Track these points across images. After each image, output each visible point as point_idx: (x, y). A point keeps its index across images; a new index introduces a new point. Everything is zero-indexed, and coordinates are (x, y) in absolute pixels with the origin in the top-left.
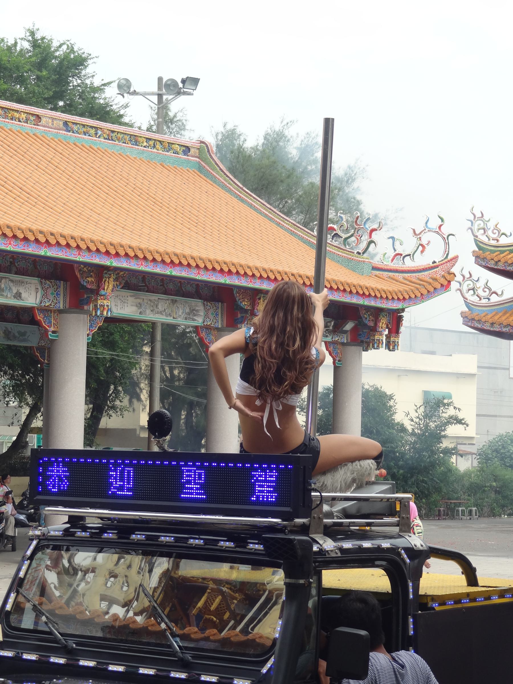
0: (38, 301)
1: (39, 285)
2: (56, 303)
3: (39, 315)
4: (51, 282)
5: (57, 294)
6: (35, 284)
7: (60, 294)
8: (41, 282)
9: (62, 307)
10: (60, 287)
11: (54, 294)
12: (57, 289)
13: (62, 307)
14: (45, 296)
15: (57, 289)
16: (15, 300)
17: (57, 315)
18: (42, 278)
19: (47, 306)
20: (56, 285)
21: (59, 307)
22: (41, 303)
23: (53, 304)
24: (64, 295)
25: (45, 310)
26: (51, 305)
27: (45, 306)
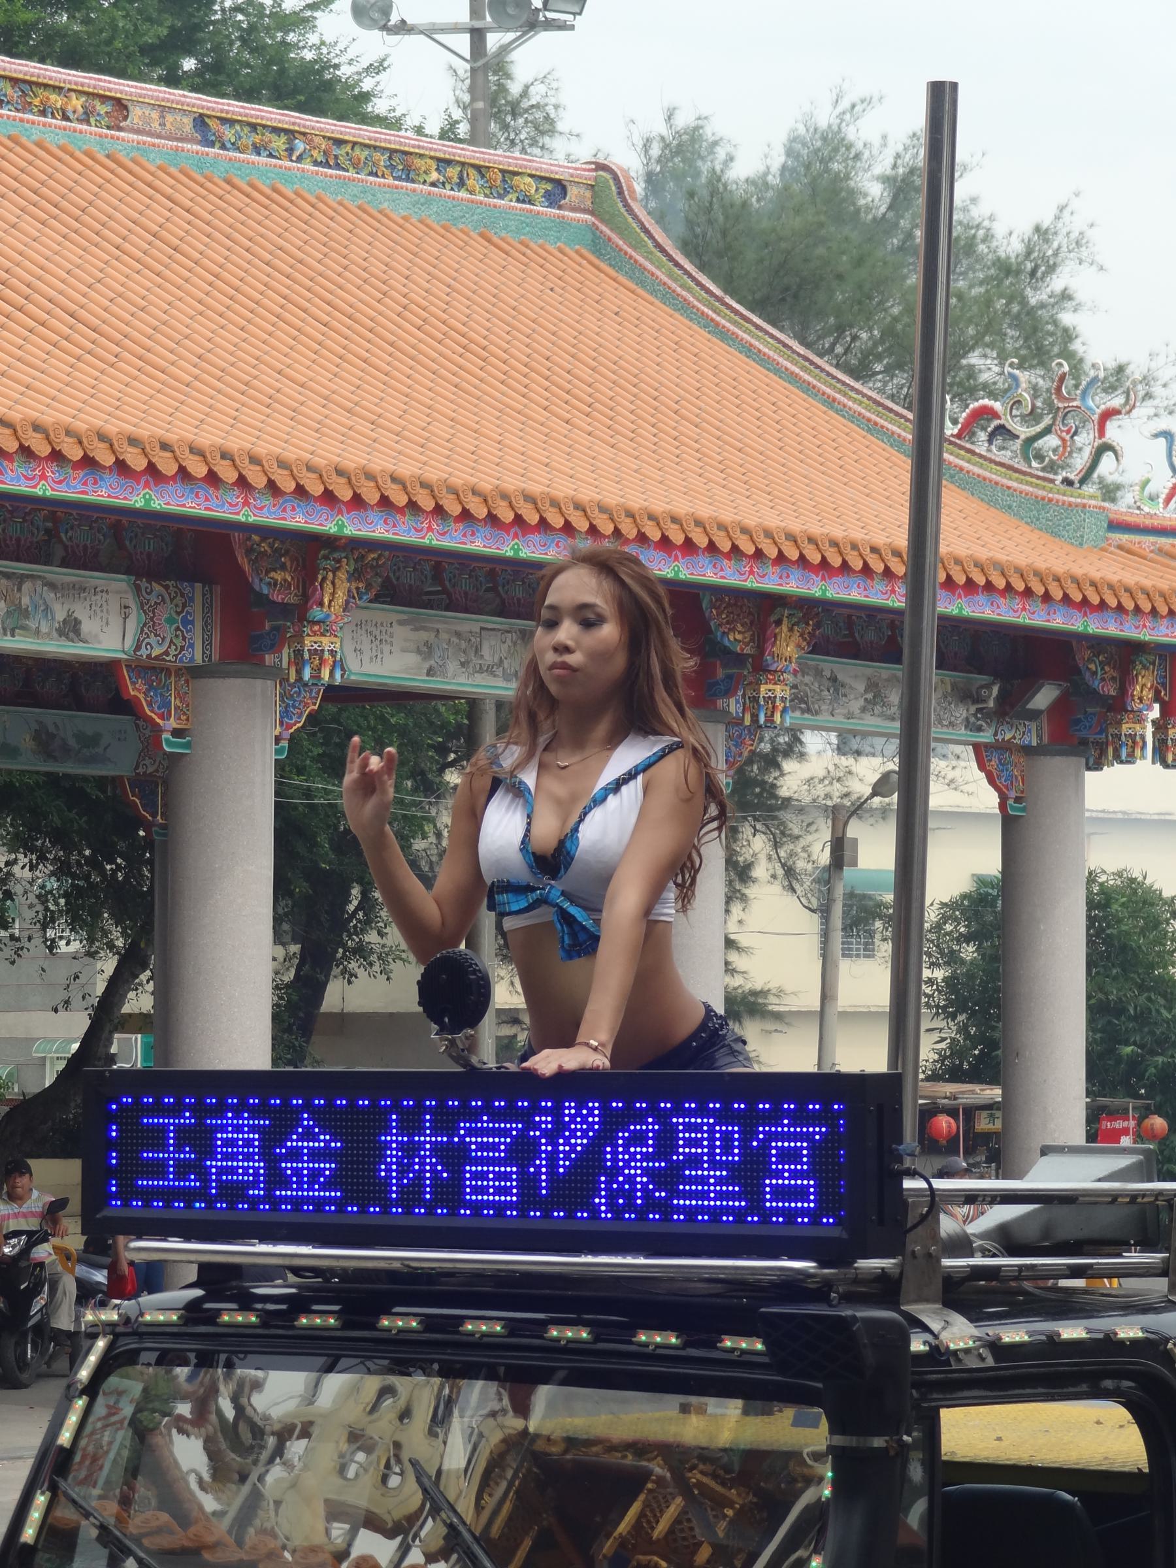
0: (129, 643)
2: (182, 648)
5: (185, 622)
7: (192, 623)
8: (138, 589)
9: (198, 659)
10: (192, 599)
11: (176, 621)
12: (184, 606)
13: (198, 659)
14: (149, 626)
15: (184, 606)
16: (63, 642)
19: (157, 658)
21: (192, 659)
22: (138, 648)
23: (172, 652)
24: (206, 624)
26: (166, 653)
27: (149, 656)
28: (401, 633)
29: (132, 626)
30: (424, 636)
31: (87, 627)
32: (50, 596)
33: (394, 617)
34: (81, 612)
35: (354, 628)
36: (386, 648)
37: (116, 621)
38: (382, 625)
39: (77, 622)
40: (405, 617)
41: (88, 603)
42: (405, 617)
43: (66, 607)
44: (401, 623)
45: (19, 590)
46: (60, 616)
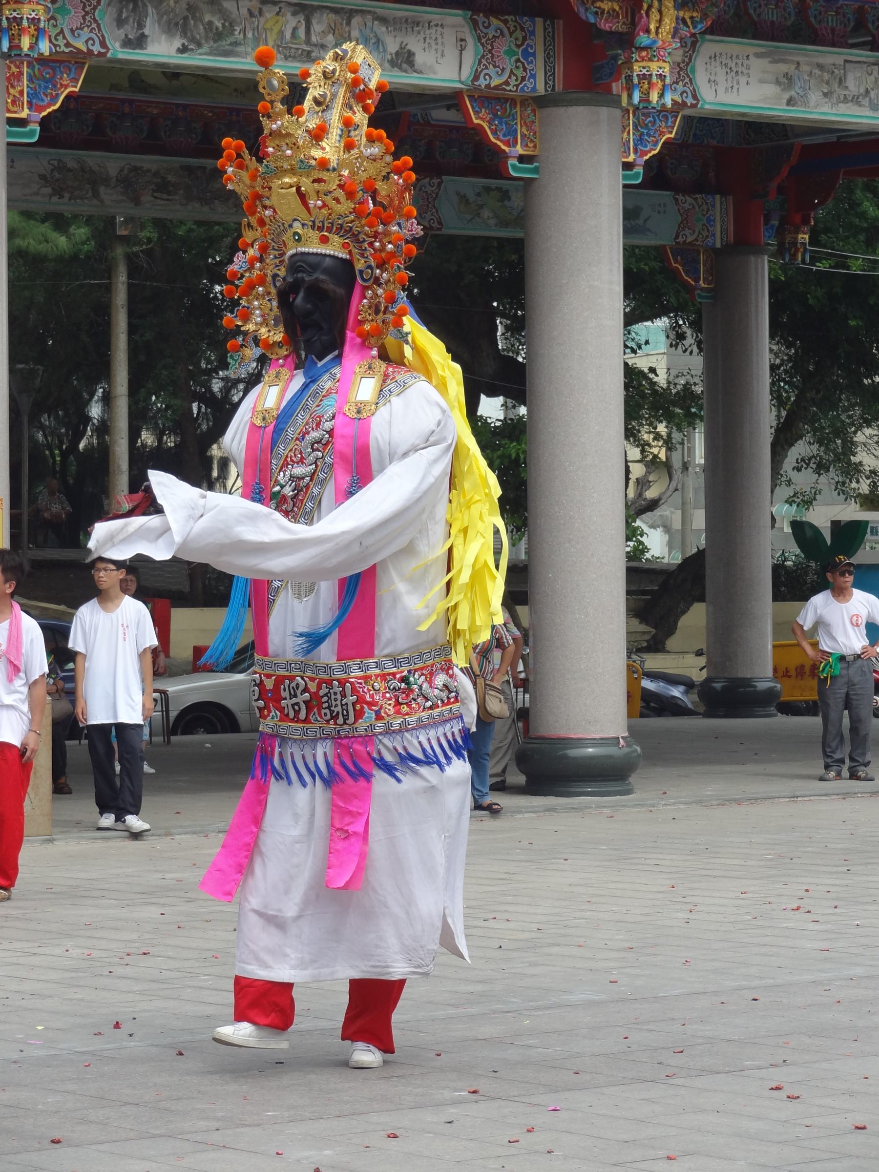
0: (467, 73)
1: (466, 29)
2: (523, 79)
3: (476, 112)
4: (505, 22)
5: (526, 54)
6: (454, 26)
7: (534, 55)
8: (475, 23)
9: (541, 89)
10: (533, 33)
11: (516, 53)
12: (525, 39)
13: (541, 89)
14: (488, 57)
15: (525, 39)
16: (396, 72)
17: (533, 111)
18: (476, 11)
19: (496, 88)
20: (522, 29)
21: (534, 89)
22: (476, 78)
23: (513, 81)
24: (548, 56)
25: (494, 100)
26: (507, 83)
27: (488, 86)
28: (758, 65)
29: (469, 58)
30: (783, 68)
31: (420, 58)
32: (381, 30)
33: (751, 50)
34: (414, 44)
35: (708, 60)
36: (743, 80)
37: (451, 53)
38: (737, 57)
39: (411, 54)
40: (763, 50)
41: (422, 36)
42: (763, 50)
43: (399, 40)
44: (758, 55)
45: (349, 23)
46: (392, 47)
